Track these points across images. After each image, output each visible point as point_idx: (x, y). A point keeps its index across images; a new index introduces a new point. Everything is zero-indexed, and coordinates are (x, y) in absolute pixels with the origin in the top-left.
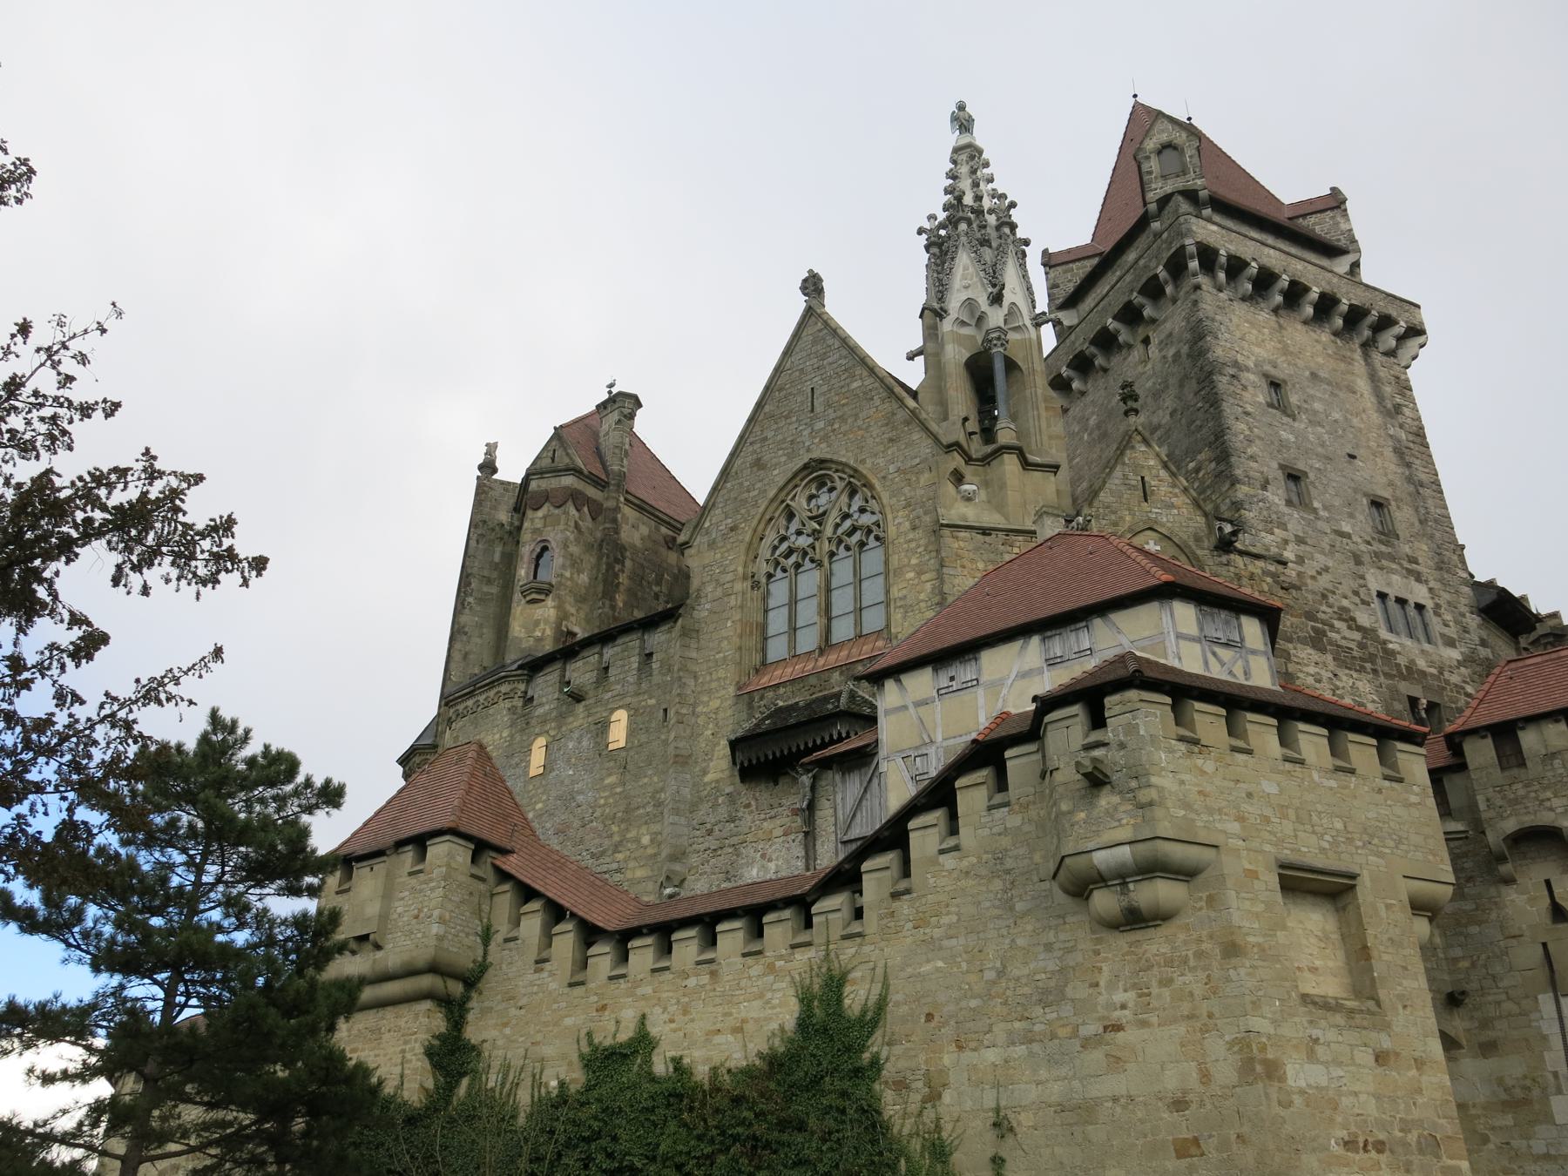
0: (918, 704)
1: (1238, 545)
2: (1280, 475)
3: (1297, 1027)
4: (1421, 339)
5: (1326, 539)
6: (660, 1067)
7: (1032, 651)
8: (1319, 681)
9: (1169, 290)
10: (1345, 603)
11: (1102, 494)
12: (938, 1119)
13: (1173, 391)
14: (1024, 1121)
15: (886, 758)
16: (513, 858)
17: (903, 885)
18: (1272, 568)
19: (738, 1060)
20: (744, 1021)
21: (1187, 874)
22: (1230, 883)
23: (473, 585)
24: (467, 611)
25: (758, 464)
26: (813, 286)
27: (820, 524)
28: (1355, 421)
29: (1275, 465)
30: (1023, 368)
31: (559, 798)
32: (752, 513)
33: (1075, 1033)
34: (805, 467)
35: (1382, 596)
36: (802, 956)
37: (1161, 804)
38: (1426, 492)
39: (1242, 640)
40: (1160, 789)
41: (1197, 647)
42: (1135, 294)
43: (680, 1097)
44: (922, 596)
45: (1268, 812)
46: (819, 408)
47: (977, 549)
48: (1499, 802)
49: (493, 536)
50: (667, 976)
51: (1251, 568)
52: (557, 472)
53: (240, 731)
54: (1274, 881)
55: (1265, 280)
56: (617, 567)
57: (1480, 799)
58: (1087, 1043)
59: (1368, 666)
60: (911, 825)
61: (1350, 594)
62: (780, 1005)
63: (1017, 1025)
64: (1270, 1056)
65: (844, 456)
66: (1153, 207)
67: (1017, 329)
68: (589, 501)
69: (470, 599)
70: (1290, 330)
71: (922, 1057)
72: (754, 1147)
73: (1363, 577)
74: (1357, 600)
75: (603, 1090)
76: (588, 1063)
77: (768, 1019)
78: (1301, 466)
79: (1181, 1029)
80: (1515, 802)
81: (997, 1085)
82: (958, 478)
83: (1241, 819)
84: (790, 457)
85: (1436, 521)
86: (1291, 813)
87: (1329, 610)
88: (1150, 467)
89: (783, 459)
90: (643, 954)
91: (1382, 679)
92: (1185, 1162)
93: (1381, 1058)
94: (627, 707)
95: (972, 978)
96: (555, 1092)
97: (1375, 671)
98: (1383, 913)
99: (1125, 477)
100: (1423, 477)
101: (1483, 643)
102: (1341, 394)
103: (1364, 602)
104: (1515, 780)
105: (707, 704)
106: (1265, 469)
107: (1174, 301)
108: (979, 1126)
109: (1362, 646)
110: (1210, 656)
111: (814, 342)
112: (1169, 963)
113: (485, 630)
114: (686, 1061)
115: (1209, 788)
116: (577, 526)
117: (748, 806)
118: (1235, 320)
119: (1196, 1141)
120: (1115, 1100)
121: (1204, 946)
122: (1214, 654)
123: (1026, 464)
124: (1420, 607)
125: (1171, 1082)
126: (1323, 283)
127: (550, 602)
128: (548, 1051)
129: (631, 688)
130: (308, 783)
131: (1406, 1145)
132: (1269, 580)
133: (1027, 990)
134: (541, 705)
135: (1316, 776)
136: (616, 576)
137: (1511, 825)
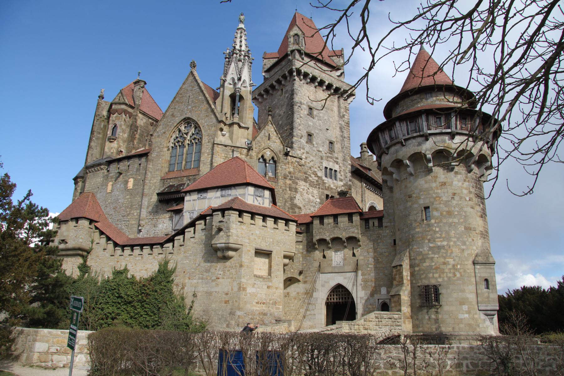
0: (194, 200)
1: (290, 154)
2: (306, 135)
3: (252, 281)
4: (354, 97)
5: (315, 152)
6: (129, 276)
7: (219, 193)
8: (303, 190)
9: (288, 78)
10: (316, 170)
11: (258, 138)
12: (183, 292)
13: (285, 106)
14: (199, 295)
15: (185, 212)
16: (99, 223)
17: (182, 243)
18: (298, 160)
19: (146, 276)
20: (148, 268)
21: (235, 250)
22: (243, 253)
23: (95, 134)
24: (93, 142)
25: (173, 115)
26: (193, 65)
27: (187, 135)
28: (331, 119)
29: (305, 132)
30: (245, 98)
31: (114, 199)
32: (170, 129)
33: (211, 279)
34: (185, 119)
35: (326, 168)
36: (160, 256)
38: (345, 140)
39: (264, 195)
40: (232, 233)
41: (252, 197)
42: (280, 77)
43: (133, 283)
44: (208, 161)
45: (256, 238)
46: (190, 102)
47: (223, 150)
48: (317, 232)
49: (101, 119)
50: (132, 256)
51: (292, 160)
52: (120, 104)
53: (36, 206)
55: (313, 79)
56: (135, 133)
57: (314, 231)
58: (213, 281)
59: (318, 186)
60: (186, 230)
61: (317, 167)
62: (156, 266)
63: (201, 276)
64: (245, 286)
65: (195, 118)
66: (289, 52)
67: (245, 87)
68: (129, 113)
69: (94, 138)
70: (318, 92)
71: (182, 280)
72: (147, 295)
73: (322, 163)
74: (319, 169)
75: (117, 280)
76: (114, 274)
77: (152, 268)
78: (312, 132)
79: (229, 280)
80: (320, 233)
81: (195, 287)
82: (222, 130)
83: (249, 239)
84: (181, 115)
85: (346, 148)
86: (261, 238)
87: (311, 172)
88: (272, 131)
89: (179, 115)
90: (128, 251)
91: (320, 190)
92: (226, 304)
93: (268, 287)
94: (133, 178)
95: (194, 265)
96: (107, 279)
97: (319, 188)
98: (277, 259)
99: (265, 133)
100: (346, 135)
101: (350, 181)
102: (329, 112)
103: (321, 170)
104: (321, 228)
105: (153, 181)
106: (302, 133)
107: (289, 81)
108: (191, 294)
109: (317, 181)
110: (255, 199)
111: (191, 82)
112: (230, 267)
113: (98, 148)
114: (135, 275)
116: (125, 120)
117: (161, 209)
118: (303, 89)
119: (228, 301)
120: (216, 292)
121: (237, 265)
122: (256, 199)
123: (240, 127)
124: (336, 171)
125: (226, 290)
126: (330, 80)
127: (116, 142)
128: (106, 269)
129: (135, 173)
130: (51, 217)
131: (269, 303)
132: (297, 163)
133: (203, 269)
134: (111, 173)
135: (269, 230)
136: (135, 135)
137: (318, 238)
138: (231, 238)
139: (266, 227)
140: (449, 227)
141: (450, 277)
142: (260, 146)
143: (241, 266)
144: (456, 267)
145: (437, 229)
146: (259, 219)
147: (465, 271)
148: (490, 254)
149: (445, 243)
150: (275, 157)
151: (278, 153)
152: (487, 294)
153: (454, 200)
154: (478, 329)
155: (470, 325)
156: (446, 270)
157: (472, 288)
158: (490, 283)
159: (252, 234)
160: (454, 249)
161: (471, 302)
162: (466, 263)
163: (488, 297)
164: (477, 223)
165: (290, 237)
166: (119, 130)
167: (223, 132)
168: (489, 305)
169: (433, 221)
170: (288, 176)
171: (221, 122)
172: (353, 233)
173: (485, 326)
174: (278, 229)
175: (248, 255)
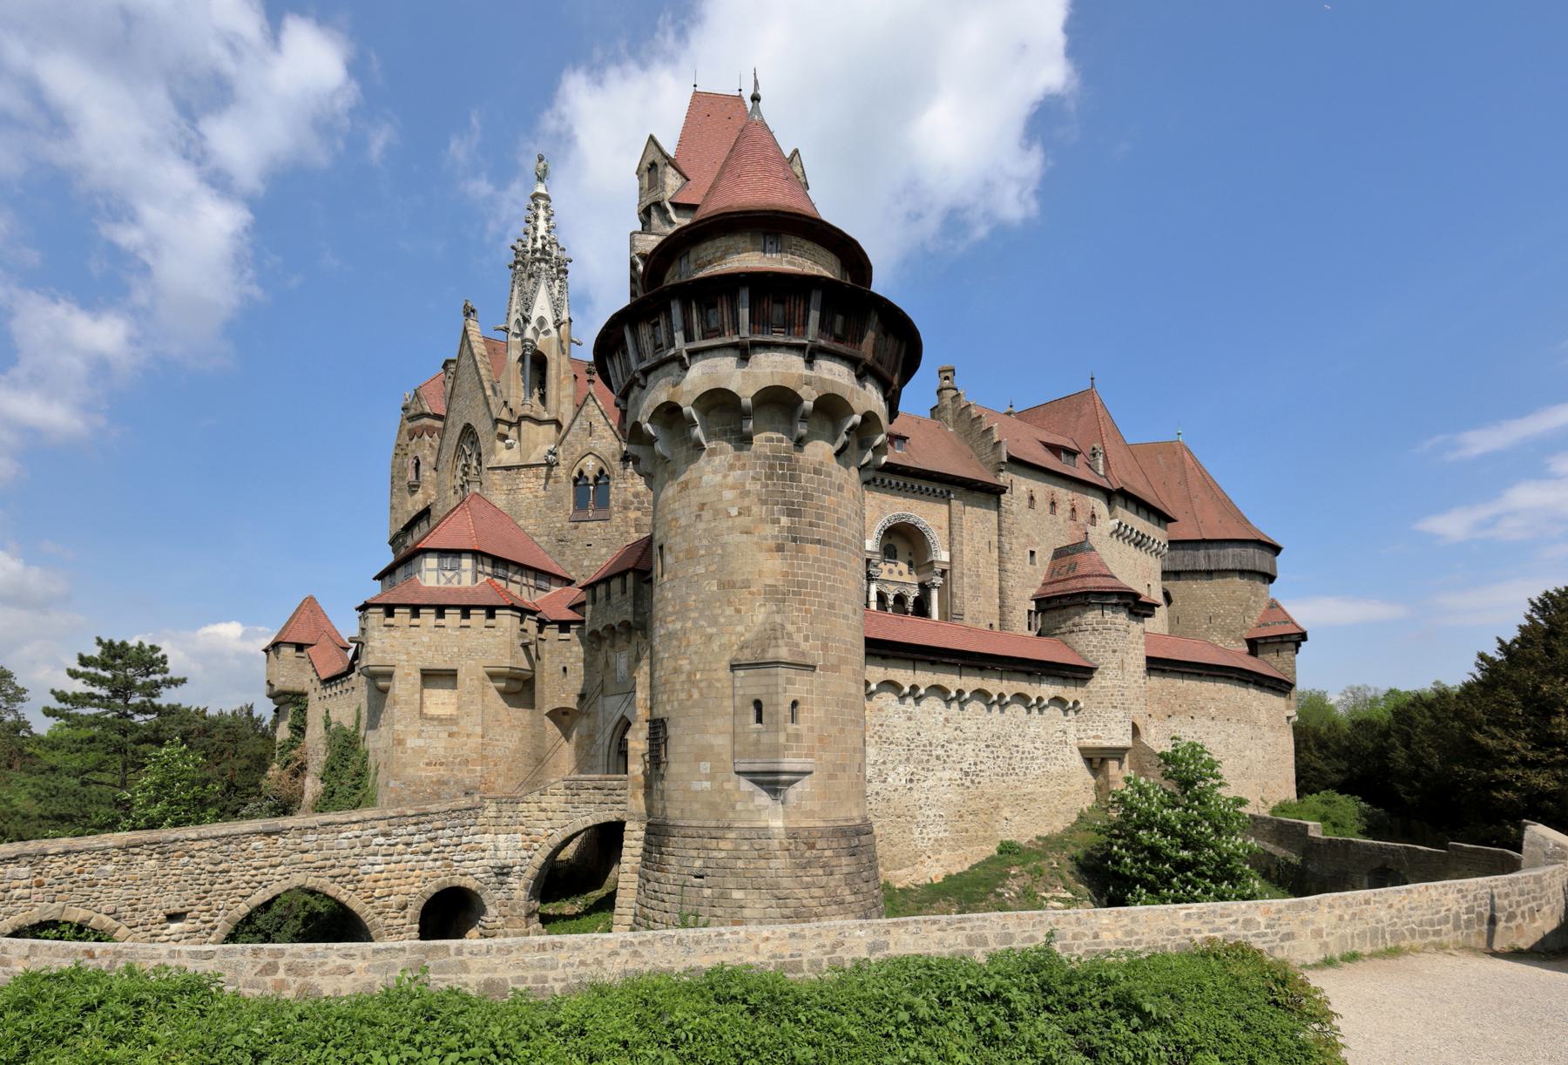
37: (373, 652)
39: (460, 566)
45: (422, 649)
54: (418, 676)
83: (408, 654)
86: (433, 649)
88: (595, 416)
98: (468, 682)
99: (581, 424)
110: (442, 578)
115: (395, 643)
116: (431, 445)
123: (539, 422)
135: (449, 631)
138: (370, 656)
139: (444, 626)
140: (687, 587)
141: (682, 700)
142: (573, 453)
143: (395, 703)
144: (693, 678)
145: (670, 595)
146: (428, 617)
147: (710, 685)
148: (773, 642)
149: (678, 625)
150: (605, 468)
151: (610, 459)
152: (755, 735)
153: (701, 521)
154: (731, 815)
155: (712, 806)
156: (678, 687)
157: (724, 723)
158: (764, 709)
159: (414, 644)
160: (692, 638)
161: (720, 754)
162: (714, 666)
163: (757, 742)
164: (772, 567)
165: (497, 639)
166: (422, 467)
167: (507, 441)
168: (758, 761)
169: (666, 576)
170: (632, 503)
171: (497, 421)
172: (626, 613)
173: (751, 807)
174: (469, 627)
175: (404, 687)
